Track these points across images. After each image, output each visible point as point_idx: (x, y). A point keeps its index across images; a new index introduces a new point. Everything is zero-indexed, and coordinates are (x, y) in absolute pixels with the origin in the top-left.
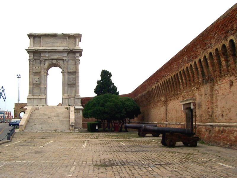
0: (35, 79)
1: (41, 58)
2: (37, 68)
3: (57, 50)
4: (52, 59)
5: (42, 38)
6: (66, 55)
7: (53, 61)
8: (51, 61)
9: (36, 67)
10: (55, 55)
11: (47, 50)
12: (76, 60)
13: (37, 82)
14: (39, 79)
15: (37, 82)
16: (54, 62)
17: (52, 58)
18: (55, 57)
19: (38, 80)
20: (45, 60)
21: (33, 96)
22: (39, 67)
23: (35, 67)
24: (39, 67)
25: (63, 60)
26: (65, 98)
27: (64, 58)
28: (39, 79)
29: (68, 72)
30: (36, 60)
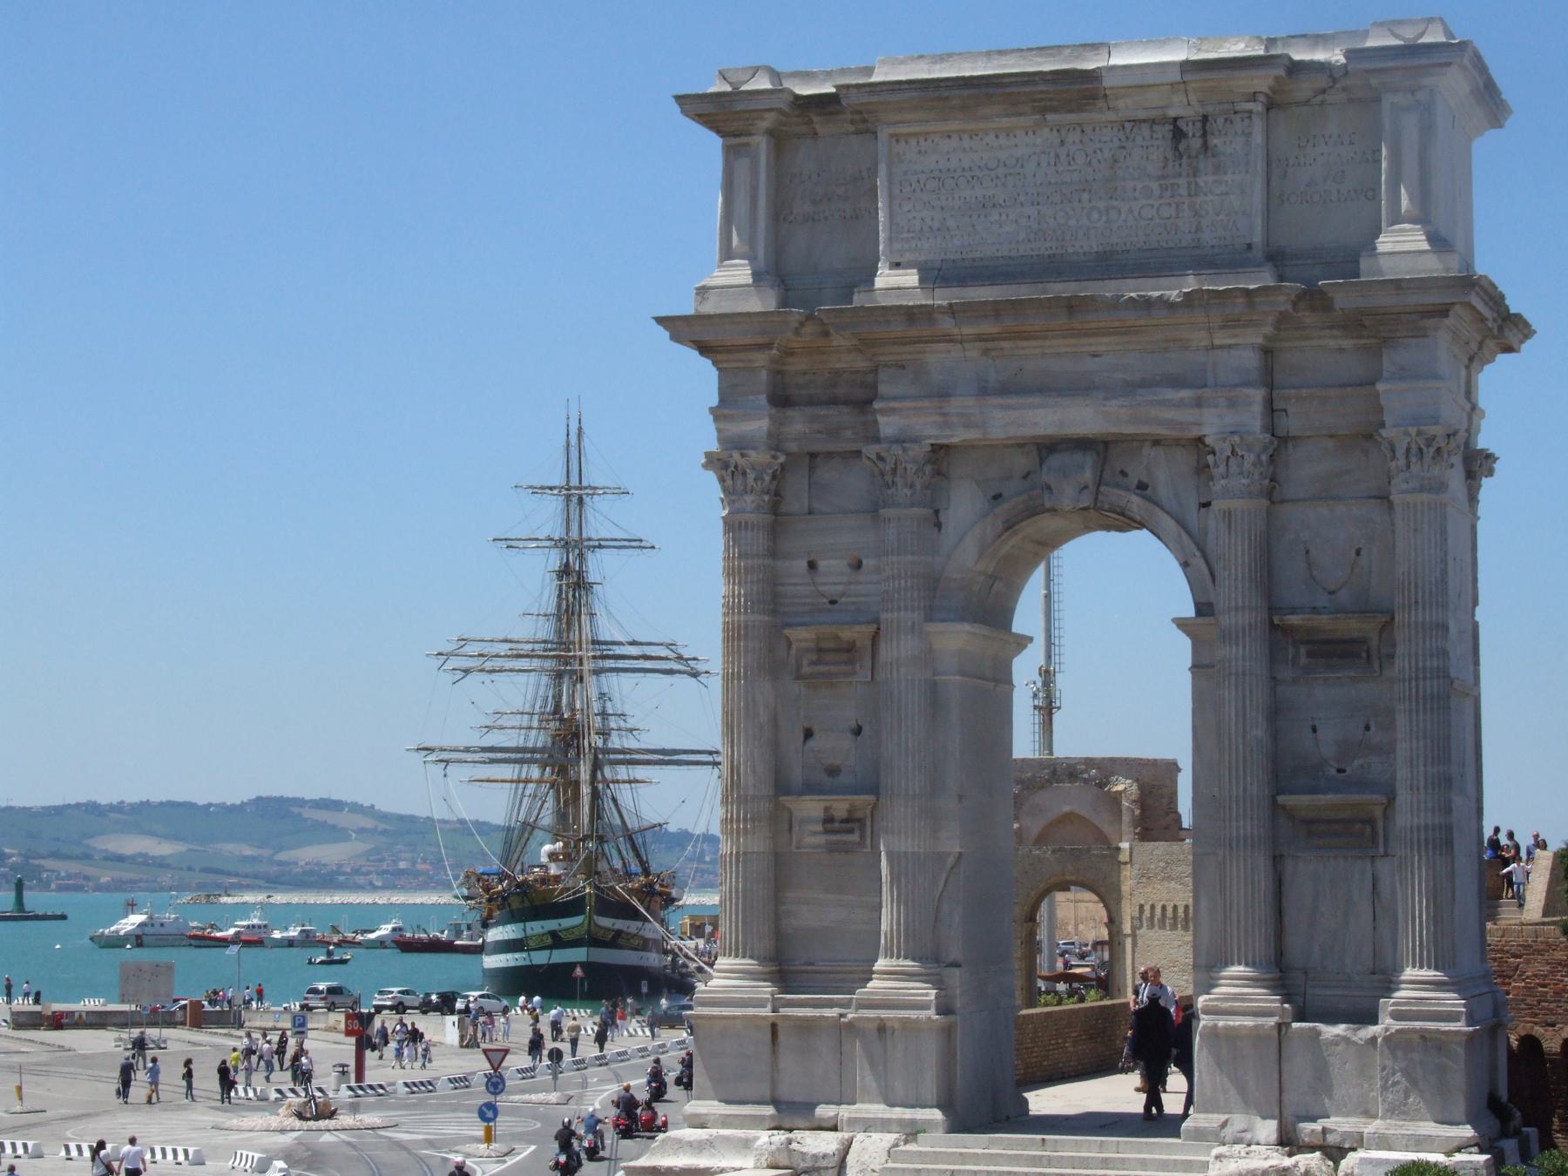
0: (808, 734)
1: (888, 425)
2: (833, 567)
4: (1048, 447)
5: (884, 133)
9: (822, 564)
10: (1079, 388)
18: (1083, 418)
19: (847, 742)
20: (940, 454)
21: (766, 990)
22: (858, 565)
23: (804, 564)
27: (1211, 424)
28: (858, 731)
30: (813, 456)
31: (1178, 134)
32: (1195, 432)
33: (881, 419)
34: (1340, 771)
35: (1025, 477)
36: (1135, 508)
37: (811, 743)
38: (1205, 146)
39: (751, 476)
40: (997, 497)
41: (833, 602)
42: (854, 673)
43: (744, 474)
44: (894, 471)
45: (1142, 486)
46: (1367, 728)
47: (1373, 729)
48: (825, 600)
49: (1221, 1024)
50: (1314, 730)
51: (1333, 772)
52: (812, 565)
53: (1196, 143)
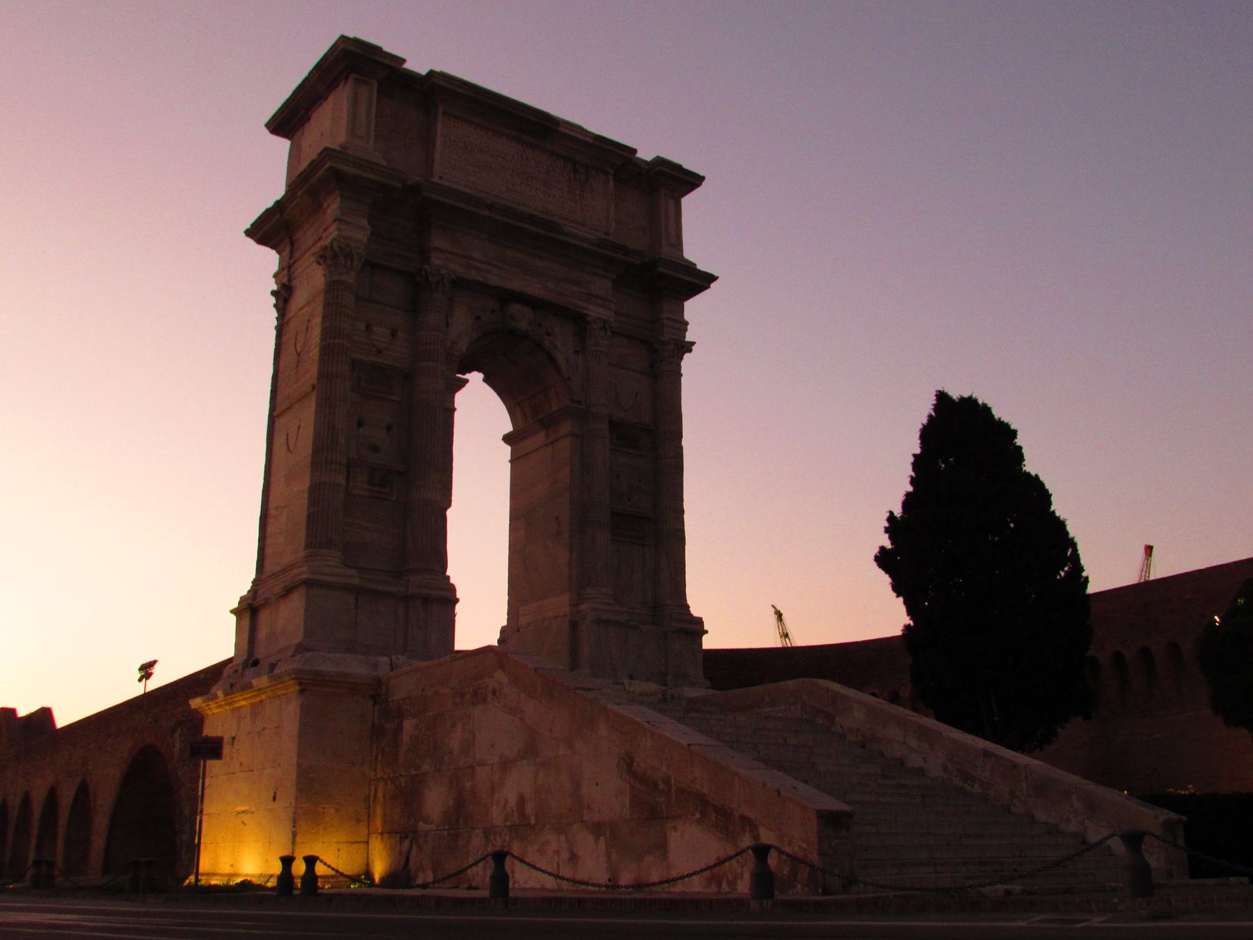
1: (437, 260)
3: (565, 239)
4: (506, 297)
5: (440, 110)
6: (602, 285)
7: (515, 308)
9: (375, 328)
11: (490, 207)
13: (375, 449)
14: (389, 428)
16: (523, 318)
17: (515, 285)
18: (535, 288)
20: (459, 284)
23: (362, 326)
24: (394, 333)
25: (579, 320)
27: (595, 311)
28: (389, 428)
29: (614, 425)
32: (585, 312)
34: (629, 500)
35: (493, 311)
36: (547, 343)
40: (478, 318)
43: (352, 260)
45: (549, 334)
48: (375, 349)
50: (618, 477)
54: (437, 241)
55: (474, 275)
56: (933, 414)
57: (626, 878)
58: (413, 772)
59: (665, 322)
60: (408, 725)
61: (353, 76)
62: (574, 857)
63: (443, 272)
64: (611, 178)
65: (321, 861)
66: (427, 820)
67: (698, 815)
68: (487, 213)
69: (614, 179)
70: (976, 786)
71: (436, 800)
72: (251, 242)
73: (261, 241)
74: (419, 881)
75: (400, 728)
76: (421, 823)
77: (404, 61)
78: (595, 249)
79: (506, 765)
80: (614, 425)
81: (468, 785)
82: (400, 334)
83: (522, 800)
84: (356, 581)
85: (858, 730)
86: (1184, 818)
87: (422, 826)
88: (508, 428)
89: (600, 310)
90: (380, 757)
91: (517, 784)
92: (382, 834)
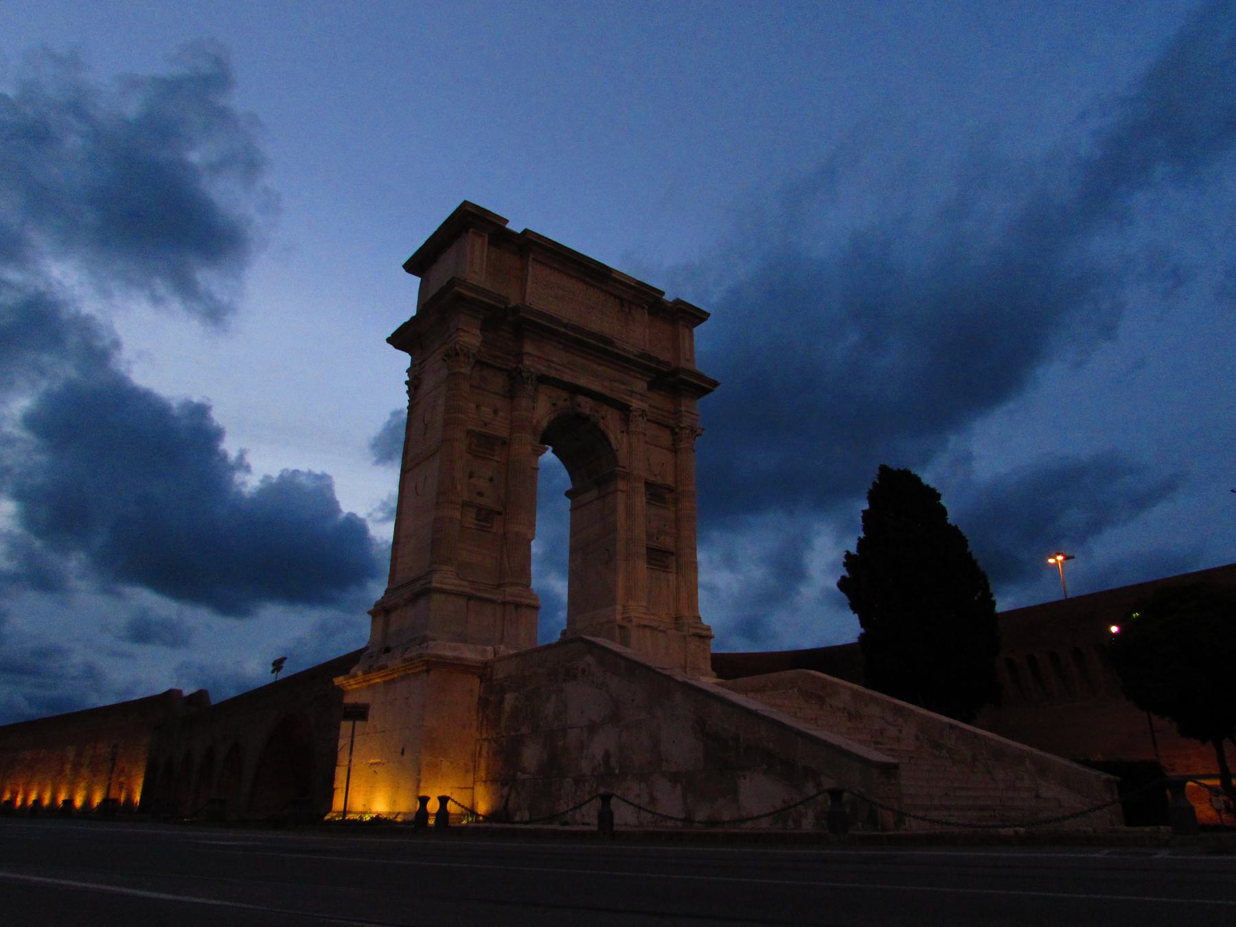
0: (471, 476)
1: (527, 362)
3: (616, 351)
4: (575, 390)
5: (531, 256)
6: (640, 385)
7: (581, 399)
8: (564, 395)
9: (483, 408)
11: (565, 326)
12: (682, 428)
13: (480, 494)
14: (491, 480)
15: (480, 494)
16: (586, 405)
17: (582, 382)
18: (595, 386)
20: (543, 380)
24: (495, 412)
25: (624, 408)
26: (645, 626)
27: (635, 404)
28: (491, 480)
29: (649, 485)
31: (622, 305)
33: (525, 357)
34: (658, 539)
35: (565, 400)
37: (473, 480)
38: (630, 312)
39: (471, 359)
41: (485, 425)
42: (493, 456)
43: (469, 358)
44: (528, 378)
45: (603, 418)
46: (665, 526)
47: (667, 527)
49: (642, 623)
51: (655, 539)
52: (478, 406)
53: (627, 310)
54: (528, 348)
55: (553, 374)
56: (878, 482)
57: (701, 816)
58: (513, 733)
59: (684, 413)
60: (509, 698)
61: (472, 230)
62: (653, 800)
63: (532, 369)
64: (646, 312)
65: (453, 800)
66: (524, 771)
67: (765, 766)
68: (563, 330)
69: (649, 314)
70: (944, 751)
71: (531, 755)
72: (390, 347)
73: (398, 346)
74: (517, 819)
75: (502, 700)
76: (519, 773)
77: (507, 221)
78: (637, 359)
79: (592, 728)
80: (649, 485)
81: (561, 743)
82: (501, 414)
83: (607, 755)
84: (467, 590)
85: (845, 708)
86: (1118, 778)
87: (520, 775)
88: (569, 486)
89: (639, 403)
90: (485, 723)
91: (602, 743)
92: (485, 782)
